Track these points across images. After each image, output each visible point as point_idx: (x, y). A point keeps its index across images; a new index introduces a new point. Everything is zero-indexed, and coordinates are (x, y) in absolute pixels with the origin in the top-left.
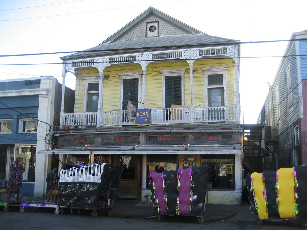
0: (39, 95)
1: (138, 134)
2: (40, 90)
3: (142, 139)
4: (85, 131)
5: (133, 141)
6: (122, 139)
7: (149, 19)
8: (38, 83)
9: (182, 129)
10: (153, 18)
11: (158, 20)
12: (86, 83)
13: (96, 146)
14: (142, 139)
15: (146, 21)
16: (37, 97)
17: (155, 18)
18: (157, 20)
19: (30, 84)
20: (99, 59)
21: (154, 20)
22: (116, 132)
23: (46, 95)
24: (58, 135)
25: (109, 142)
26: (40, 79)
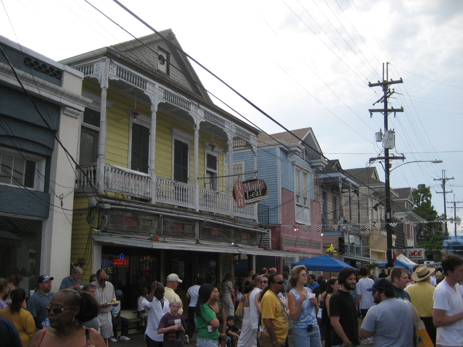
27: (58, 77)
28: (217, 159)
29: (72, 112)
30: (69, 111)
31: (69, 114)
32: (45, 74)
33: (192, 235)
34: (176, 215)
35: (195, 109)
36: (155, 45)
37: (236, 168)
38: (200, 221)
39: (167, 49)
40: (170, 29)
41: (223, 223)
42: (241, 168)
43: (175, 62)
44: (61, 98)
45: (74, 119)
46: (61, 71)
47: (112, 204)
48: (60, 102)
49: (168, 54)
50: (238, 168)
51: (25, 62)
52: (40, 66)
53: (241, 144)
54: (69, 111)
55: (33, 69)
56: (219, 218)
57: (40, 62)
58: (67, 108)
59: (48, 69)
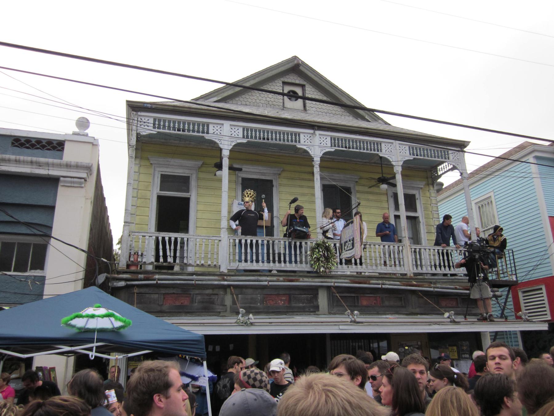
0: (62, 179)
1: (313, 291)
2: (60, 166)
3: (323, 300)
4: (195, 277)
5: (304, 305)
6: (281, 300)
7: (287, 76)
8: (54, 148)
9: (398, 283)
10: (295, 78)
11: (302, 82)
12: (156, 173)
13: (218, 314)
14: (323, 300)
15: (283, 79)
16: (54, 181)
17: (299, 78)
18: (302, 82)
19: (28, 148)
20: (223, 124)
21: (297, 82)
22: (270, 283)
23: (83, 180)
24: (122, 284)
25: (252, 305)
26: (64, 141)
27: (60, 148)
28: (417, 196)
29: (71, 182)
30: (65, 182)
31: (69, 185)
32: (40, 150)
33: (314, 309)
34: (266, 283)
35: (309, 139)
36: (276, 81)
37: (486, 203)
38: (329, 288)
39: (298, 81)
40: (295, 58)
41: (380, 286)
42: (491, 202)
43: (315, 93)
44: (48, 169)
45: (80, 189)
46: (63, 142)
47: (126, 280)
48: (48, 175)
49: (303, 86)
50: (488, 203)
51: (13, 143)
52: (33, 144)
53: (448, 169)
54: (65, 182)
55: (24, 149)
56: (374, 279)
57: (32, 140)
58: (62, 179)
59: (44, 143)
